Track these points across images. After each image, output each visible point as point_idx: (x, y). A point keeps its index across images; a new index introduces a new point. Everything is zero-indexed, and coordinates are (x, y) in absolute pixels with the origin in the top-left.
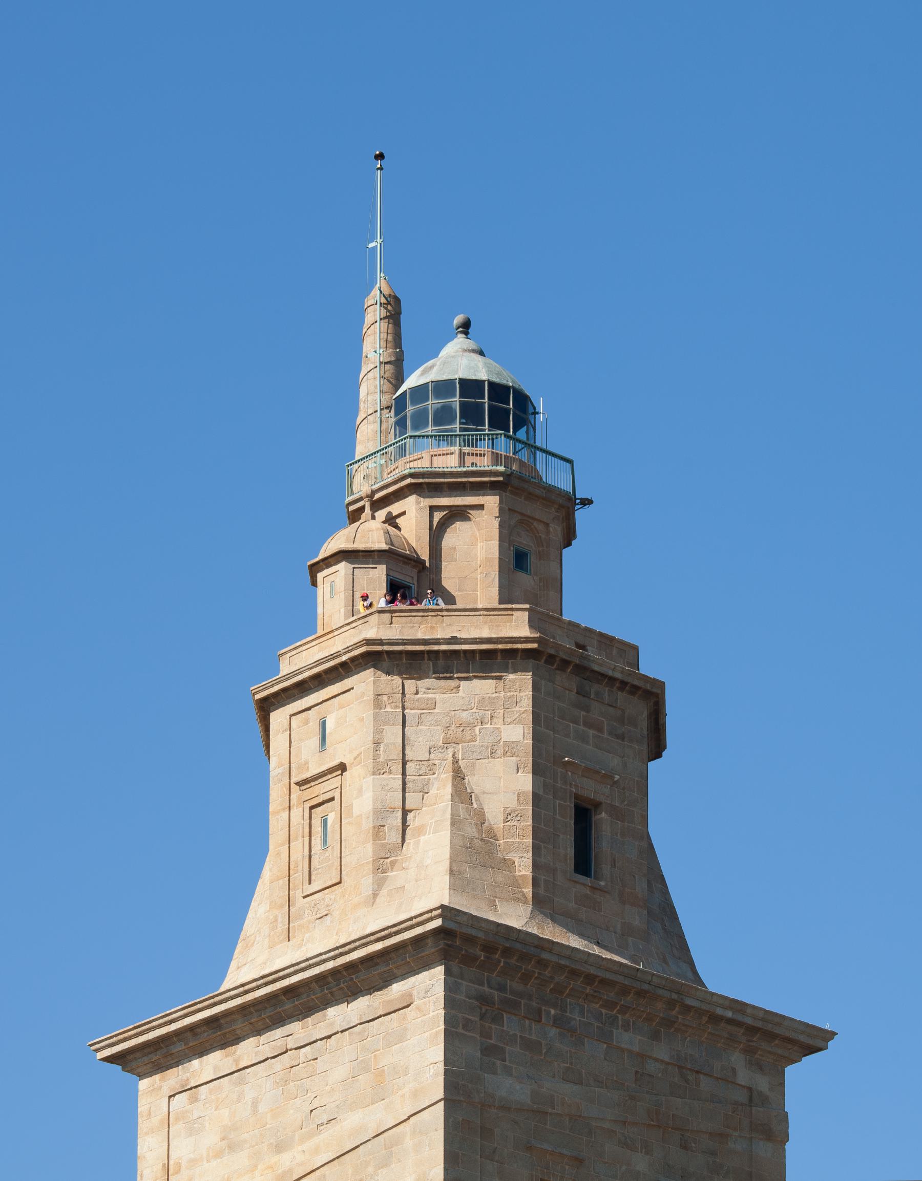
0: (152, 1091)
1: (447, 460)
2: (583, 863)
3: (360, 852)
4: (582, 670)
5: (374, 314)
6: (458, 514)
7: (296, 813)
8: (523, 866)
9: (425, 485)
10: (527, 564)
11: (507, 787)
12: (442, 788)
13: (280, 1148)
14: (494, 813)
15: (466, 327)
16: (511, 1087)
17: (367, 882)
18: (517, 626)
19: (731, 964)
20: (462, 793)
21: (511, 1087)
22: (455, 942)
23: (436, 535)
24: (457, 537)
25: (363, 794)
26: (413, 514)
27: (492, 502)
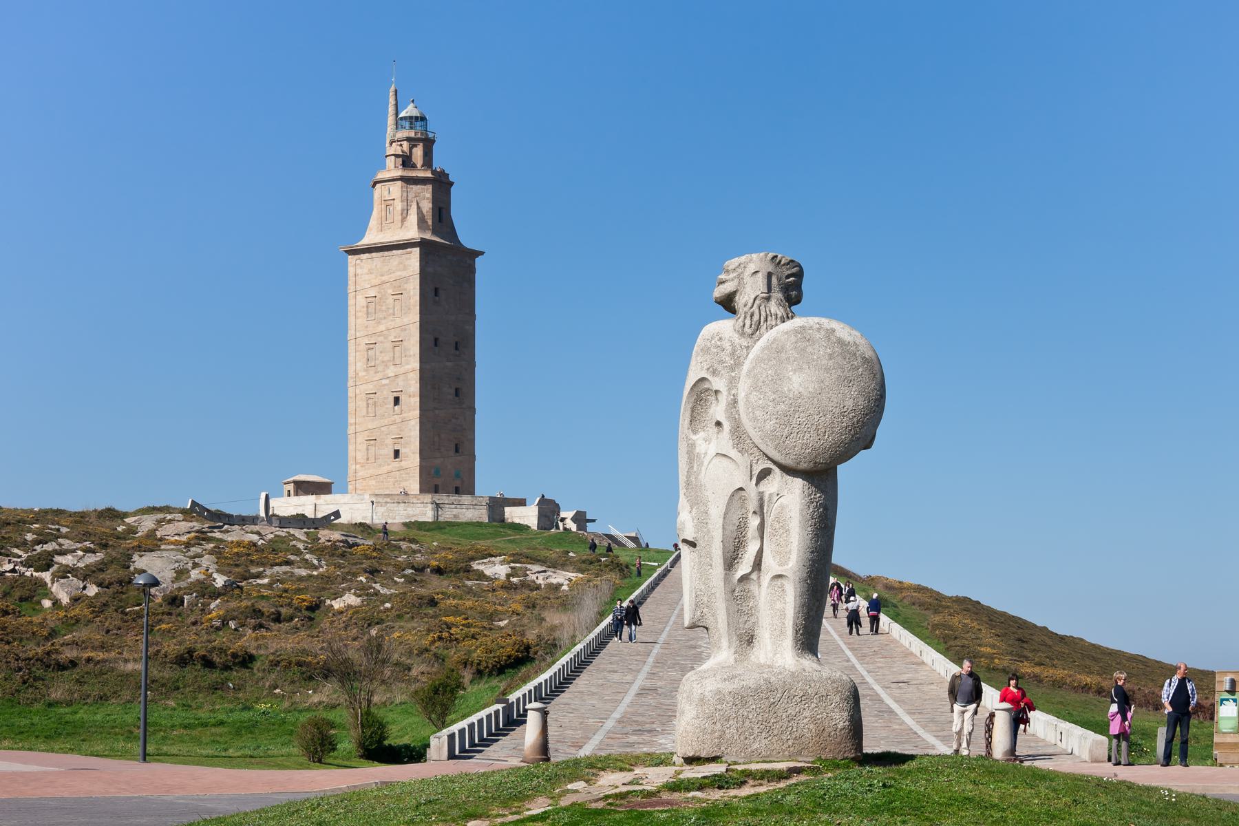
0: (352, 259)
1: (412, 135)
2: (440, 221)
4: (441, 182)
5: (392, 94)
6: (415, 146)
8: (430, 222)
9: (408, 139)
10: (428, 155)
11: (427, 206)
12: (414, 206)
14: (424, 211)
16: (430, 270)
18: (429, 174)
19: (467, 239)
20: (418, 207)
21: (430, 270)
22: (423, 244)
24: (414, 150)
25: (399, 206)
26: (406, 145)
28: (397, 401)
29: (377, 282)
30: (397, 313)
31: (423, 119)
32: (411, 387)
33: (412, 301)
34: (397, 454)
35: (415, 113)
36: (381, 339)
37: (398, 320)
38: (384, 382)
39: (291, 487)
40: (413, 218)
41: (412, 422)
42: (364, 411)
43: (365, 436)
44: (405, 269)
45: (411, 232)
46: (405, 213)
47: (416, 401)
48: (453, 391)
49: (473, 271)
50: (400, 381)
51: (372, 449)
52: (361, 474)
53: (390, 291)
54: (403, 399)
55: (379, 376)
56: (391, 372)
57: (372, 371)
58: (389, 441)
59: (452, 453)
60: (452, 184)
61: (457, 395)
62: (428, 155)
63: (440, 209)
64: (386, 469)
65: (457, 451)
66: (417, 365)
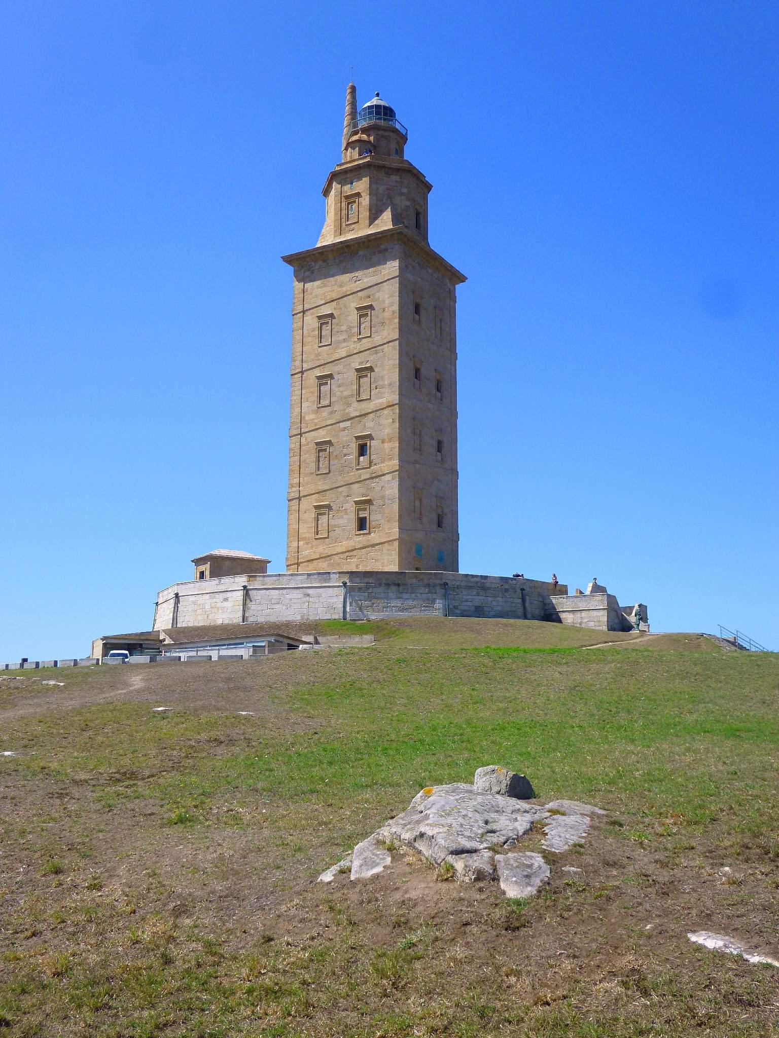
3: (365, 214)
7: (343, 204)
13: (341, 286)
15: (378, 95)
17: (367, 222)
27: (391, 134)
29: (334, 295)
33: (387, 314)
34: (362, 524)
36: (338, 368)
37: (364, 341)
38: (342, 425)
39: (206, 568)
41: (388, 478)
42: (313, 466)
43: (313, 501)
47: (393, 447)
48: (435, 444)
49: (454, 300)
50: (369, 422)
51: (323, 520)
53: (354, 305)
55: (337, 417)
56: (354, 409)
57: (325, 413)
58: (350, 506)
59: (435, 526)
60: (429, 187)
61: (439, 449)
63: (418, 214)
65: (439, 525)
66: (395, 398)
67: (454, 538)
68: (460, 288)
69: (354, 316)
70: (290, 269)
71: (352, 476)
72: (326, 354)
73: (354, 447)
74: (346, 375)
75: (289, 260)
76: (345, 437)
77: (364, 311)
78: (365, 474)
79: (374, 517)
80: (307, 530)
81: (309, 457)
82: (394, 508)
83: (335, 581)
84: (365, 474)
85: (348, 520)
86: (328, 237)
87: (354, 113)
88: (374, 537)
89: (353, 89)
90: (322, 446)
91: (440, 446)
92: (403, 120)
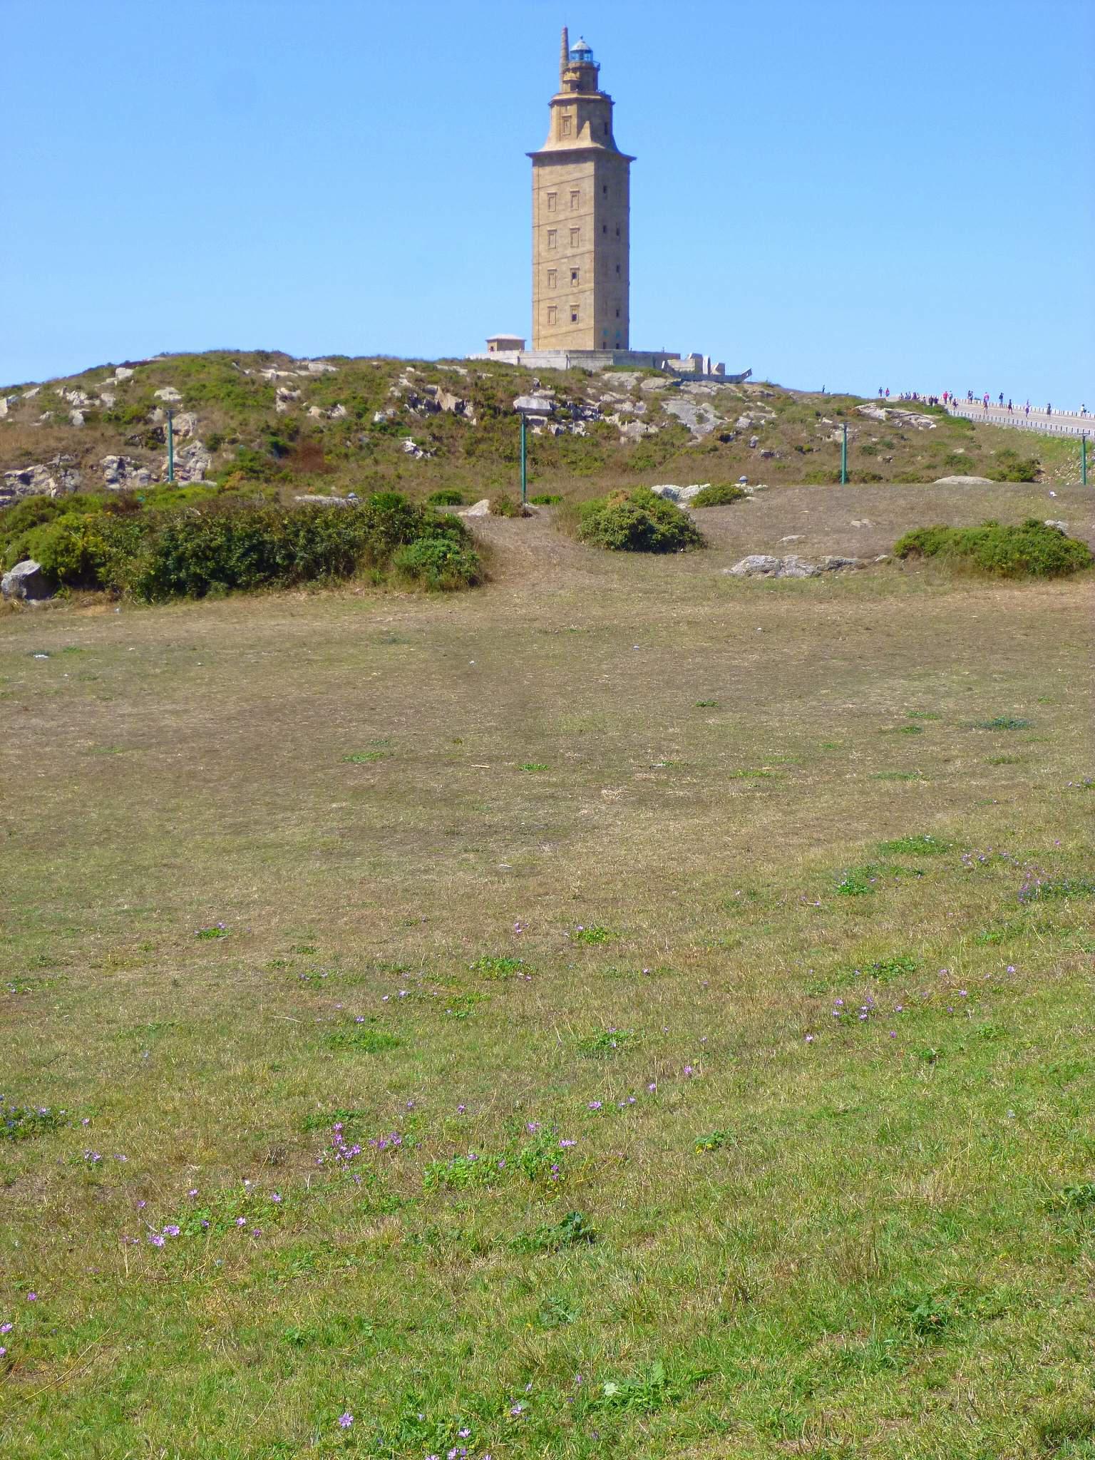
3: (574, 130)
19: (623, 146)
23: (582, 75)
25: (575, 121)
28: (574, 276)
30: (575, 206)
31: (589, 51)
32: (587, 266)
34: (574, 318)
35: (585, 48)
39: (495, 345)
40: (587, 130)
44: (581, 171)
45: (586, 142)
46: (580, 127)
49: (628, 173)
50: (577, 260)
51: (553, 314)
52: (543, 333)
54: (580, 274)
56: (569, 252)
57: (553, 252)
58: (567, 308)
62: (595, 80)
63: (606, 125)
64: (564, 329)
66: (592, 247)
67: (627, 320)
68: (632, 165)
69: (569, 196)
70: (530, 160)
71: (568, 291)
72: (552, 217)
73: (569, 274)
74: (564, 232)
75: (530, 155)
76: (564, 268)
77: (574, 194)
78: (575, 290)
79: (580, 315)
80: (543, 319)
81: (544, 278)
82: (591, 311)
83: (563, 355)
84: (575, 290)
85: (566, 316)
86: (551, 146)
87: (567, 57)
88: (581, 326)
89: (566, 30)
90: (551, 272)
91: (618, 268)
92: (597, 58)
